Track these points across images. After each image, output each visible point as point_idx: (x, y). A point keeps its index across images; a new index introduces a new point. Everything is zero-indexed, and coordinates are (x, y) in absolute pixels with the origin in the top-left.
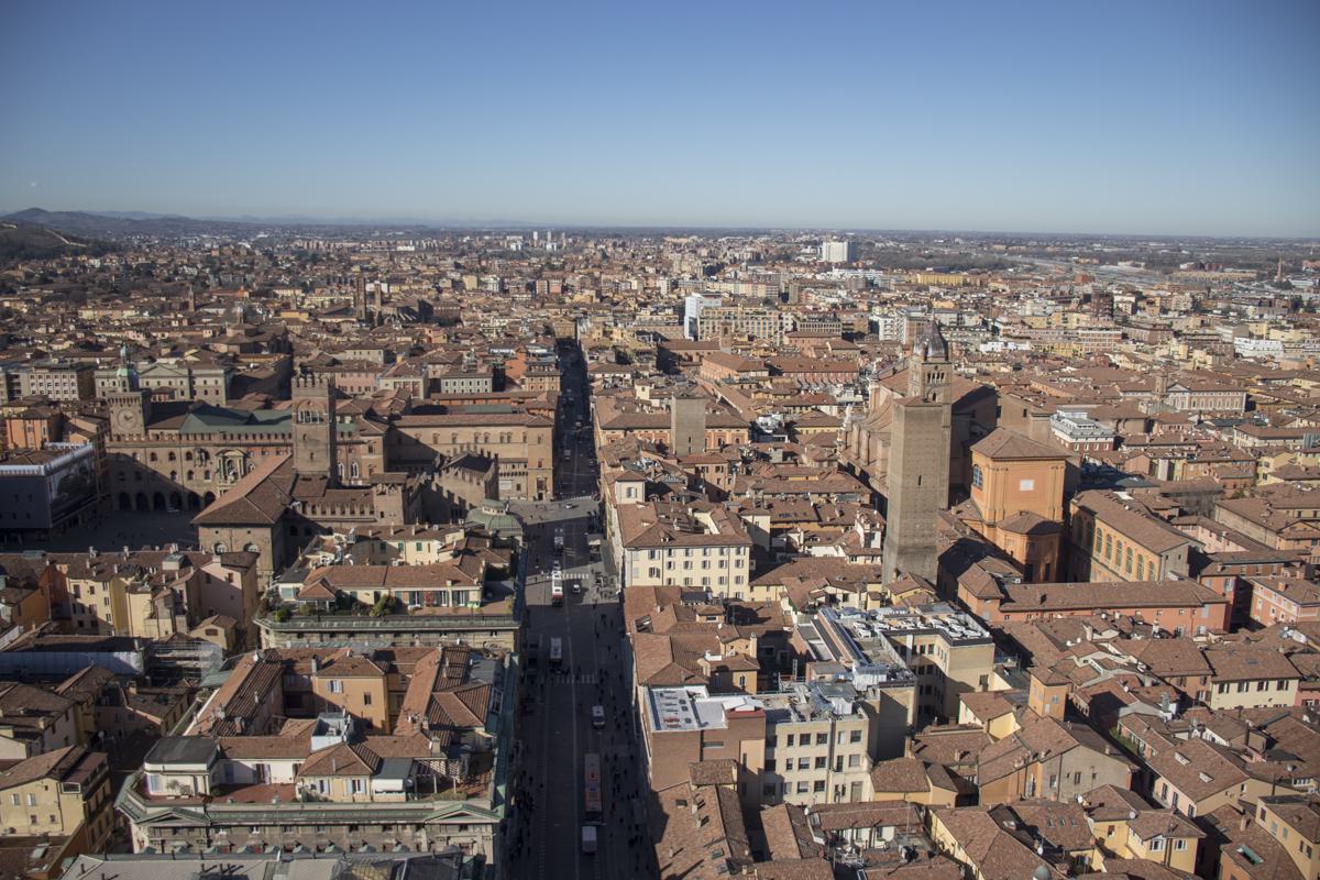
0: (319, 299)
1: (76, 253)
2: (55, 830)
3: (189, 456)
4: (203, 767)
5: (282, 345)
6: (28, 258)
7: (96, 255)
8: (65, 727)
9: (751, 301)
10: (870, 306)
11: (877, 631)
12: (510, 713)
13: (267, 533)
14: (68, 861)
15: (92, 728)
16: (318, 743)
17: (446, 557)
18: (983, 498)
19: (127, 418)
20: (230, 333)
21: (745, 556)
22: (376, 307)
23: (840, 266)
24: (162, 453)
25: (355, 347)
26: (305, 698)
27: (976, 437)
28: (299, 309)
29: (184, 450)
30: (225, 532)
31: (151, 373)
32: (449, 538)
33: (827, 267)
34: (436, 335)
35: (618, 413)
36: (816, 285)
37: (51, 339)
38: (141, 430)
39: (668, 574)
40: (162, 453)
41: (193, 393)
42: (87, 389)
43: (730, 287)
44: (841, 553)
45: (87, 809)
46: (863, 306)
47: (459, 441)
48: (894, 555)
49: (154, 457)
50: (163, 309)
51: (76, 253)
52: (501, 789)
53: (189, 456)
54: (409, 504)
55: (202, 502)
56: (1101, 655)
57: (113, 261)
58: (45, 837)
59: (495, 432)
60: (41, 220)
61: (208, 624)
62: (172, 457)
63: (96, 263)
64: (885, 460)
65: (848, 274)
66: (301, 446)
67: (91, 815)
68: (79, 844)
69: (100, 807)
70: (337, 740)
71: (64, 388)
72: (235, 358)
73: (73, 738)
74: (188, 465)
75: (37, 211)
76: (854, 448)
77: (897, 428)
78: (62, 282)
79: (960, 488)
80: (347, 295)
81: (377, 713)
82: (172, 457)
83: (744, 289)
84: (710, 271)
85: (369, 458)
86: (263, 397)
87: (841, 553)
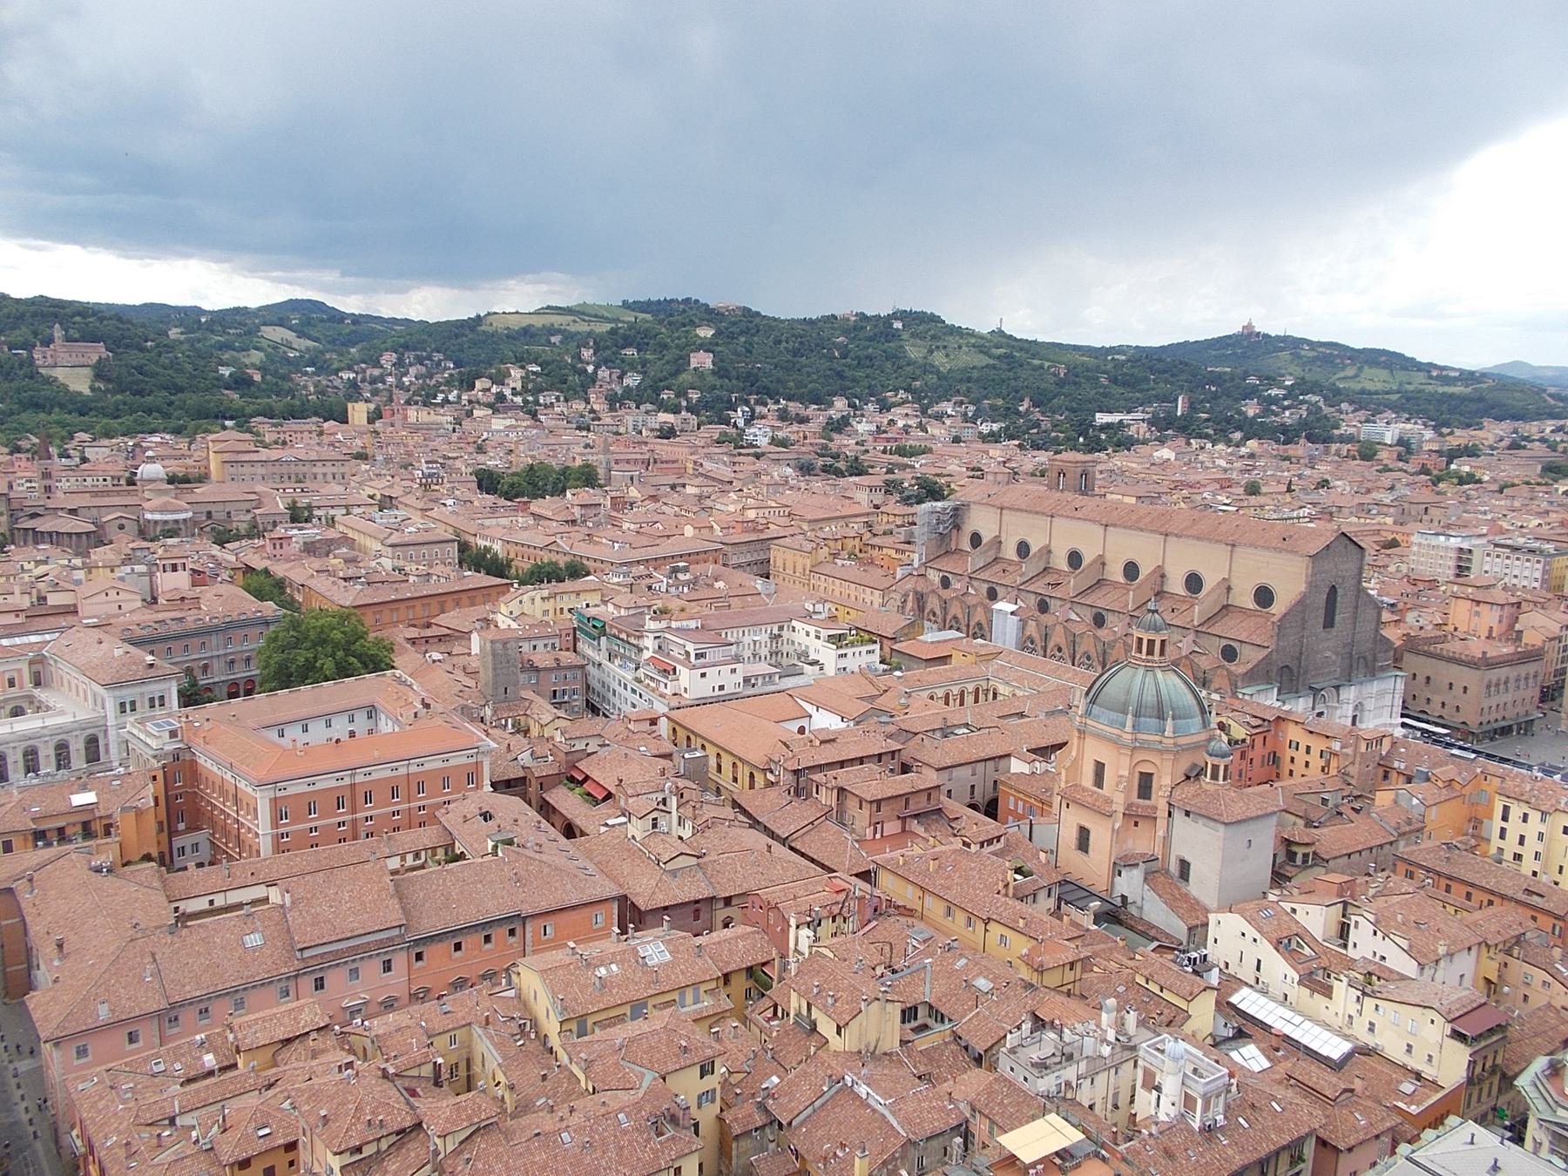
2: (1428, 1072)
58: (1418, 1076)
73: (1467, 982)
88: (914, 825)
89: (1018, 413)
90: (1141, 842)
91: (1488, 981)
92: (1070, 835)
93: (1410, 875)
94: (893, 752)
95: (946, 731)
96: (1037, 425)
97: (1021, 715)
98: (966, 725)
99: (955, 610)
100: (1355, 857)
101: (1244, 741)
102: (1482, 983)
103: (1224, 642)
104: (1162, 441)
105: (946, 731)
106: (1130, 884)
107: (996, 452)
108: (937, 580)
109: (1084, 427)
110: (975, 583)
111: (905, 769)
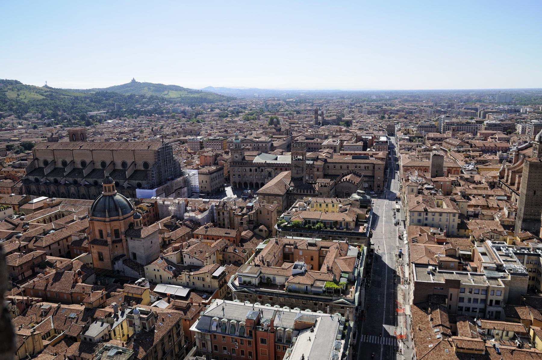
8: (214, 258)
11: (511, 252)
12: (362, 268)
13: (280, 198)
15: (221, 259)
19: (236, 157)
26: (290, 255)
29: (254, 168)
30: (266, 197)
31: (245, 141)
47: (349, 168)
48: (520, 222)
54: (331, 190)
55: (260, 186)
60: (212, 90)
62: (251, 170)
64: (519, 183)
66: (294, 168)
75: (210, 87)
76: (505, 178)
82: (251, 170)
86: (281, 150)
88: (37, 269)
89: (58, 115)
90: (119, 251)
91: (221, 260)
92: (96, 256)
93: (197, 238)
94: (25, 246)
95: (45, 233)
96: (66, 119)
97: (73, 221)
98: (53, 229)
99: (43, 189)
100: (183, 237)
101: (147, 211)
102: (219, 262)
103: (137, 182)
105: (45, 233)
106: (119, 265)
108: (33, 180)
110: (49, 178)
111: (31, 250)
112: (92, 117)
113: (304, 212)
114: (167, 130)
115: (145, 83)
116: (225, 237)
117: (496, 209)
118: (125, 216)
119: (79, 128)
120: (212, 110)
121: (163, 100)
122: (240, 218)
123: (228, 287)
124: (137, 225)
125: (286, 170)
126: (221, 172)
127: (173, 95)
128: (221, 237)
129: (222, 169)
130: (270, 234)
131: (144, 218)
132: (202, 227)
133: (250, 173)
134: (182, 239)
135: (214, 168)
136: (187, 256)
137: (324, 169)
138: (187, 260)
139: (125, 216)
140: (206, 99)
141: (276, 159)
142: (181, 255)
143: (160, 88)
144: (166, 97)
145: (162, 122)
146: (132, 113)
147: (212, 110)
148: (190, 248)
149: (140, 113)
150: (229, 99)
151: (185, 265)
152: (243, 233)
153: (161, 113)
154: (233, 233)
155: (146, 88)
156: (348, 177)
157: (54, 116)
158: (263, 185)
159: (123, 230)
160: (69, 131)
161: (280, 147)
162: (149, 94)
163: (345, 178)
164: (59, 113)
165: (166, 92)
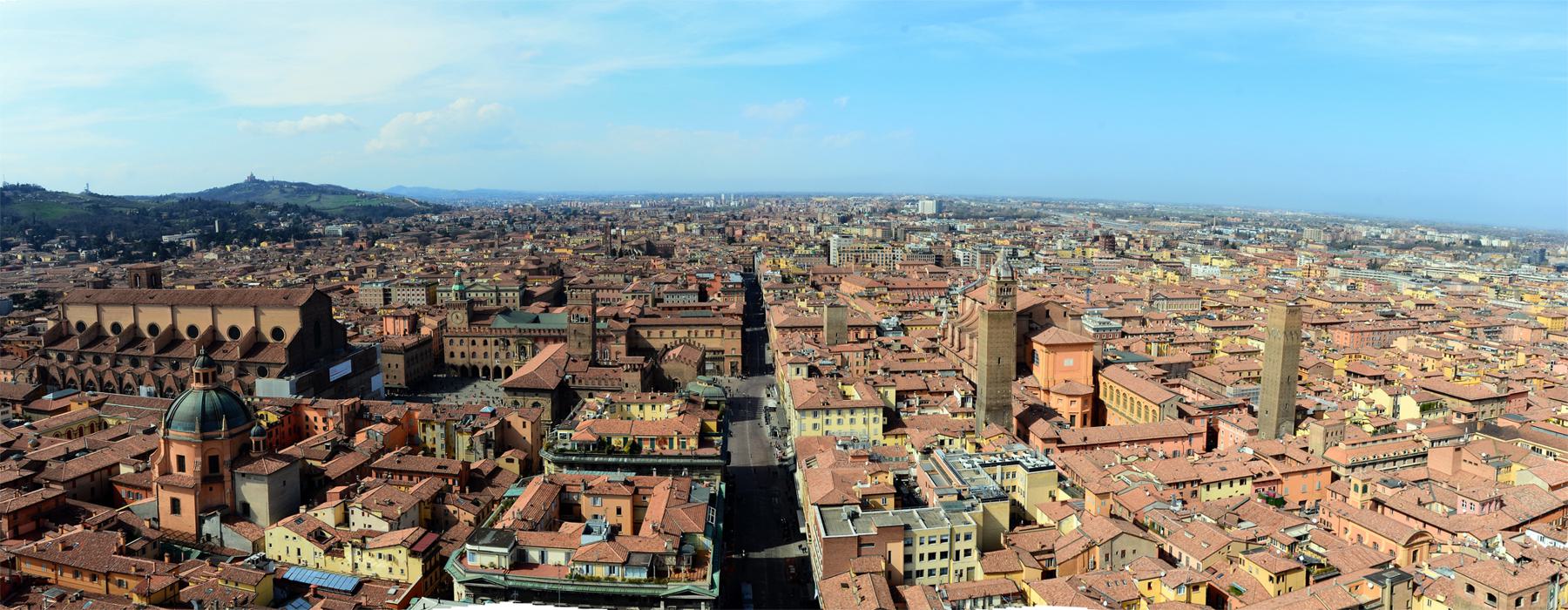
0: (577, 240)
1: (423, 212)
3: (496, 343)
4: (505, 550)
5: (555, 269)
6: (395, 216)
7: (436, 213)
8: (414, 515)
9: (871, 240)
10: (954, 243)
14: (414, 600)
16: (586, 539)
17: (673, 415)
18: (1040, 372)
20: (522, 262)
21: (880, 416)
22: (617, 246)
23: (931, 216)
24: (479, 341)
25: (606, 272)
27: (1035, 331)
28: (566, 246)
32: (675, 403)
33: (923, 217)
34: (659, 263)
35: (786, 317)
36: (914, 230)
37: (409, 266)
38: (465, 325)
39: (826, 428)
40: (479, 341)
41: (499, 302)
42: (432, 300)
43: (857, 231)
44: (946, 412)
45: (424, 568)
46: (949, 244)
48: (983, 412)
49: (474, 343)
50: (479, 247)
51: (423, 212)
52: (716, 576)
53: (496, 343)
56: (1129, 473)
57: (446, 217)
59: (702, 332)
61: (507, 454)
62: (485, 343)
63: (436, 218)
65: (937, 222)
67: (426, 573)
68: (419, 591)
69: (432, 569)
70: (600, 538)
71: (418, 298)
72: (525, 279)
74: (495, 349)
76: (949, 340)
77: (983, 327)
78: (415, 231)
79: (1025, 366)
80: (597, 237)
81: (626, 521)
82: (485, 343)
83: (868, 232)
84: (844, 220)
85: (618, 347)
86: (543, 304)
87: (946, 412)
96: (122, 247)
104: (209, 250)
107: (94, 269)
109: (157, 245)
112: (171, 244)
113: (597, 422)
114: (318, 268)
115: (273, 183)
116: (436, 474)
117: (941, 393)
118: (234, 431)
119: (149, 265)
120: (405, 230)
121: (308, 211)
122: (467, 437)
123: (444, 573)
124: (258, 448)
125: (556, 340)
126: (427, 347)
127: (328, 203)
128: (428, 474)
129: (428, 340)
130: (530, 468)
131: (270, 435)
132: (388, 455)
133: (483, 349)
134: (352, 479)
135: (411, 340)
136: (358, 512)
137: (629, 339)
138: (359, 520)
139: (234, 431)
140: (392, 209)
141: (536, 320)
142: (346, 509)
143: (304, 189)
144: (313, 206)
145: (307, 254)
146: (249, 235)
147: (405, 230)
148: (364, 496)
149: (262, 236)
150: (438, 209)
151: (354, 529)
152: (473, 467)
153: (310, 237)
154: (455, 467)
155: (276, 192)
156: (677, 351)
157: (102, 242)
158: (509, 372)
159: (227, 458)
160: (130, 269)
161: (542, 298)
162: (281, 201)
163: (671, 353)
164: (111, 238)
165: (315, 198)
